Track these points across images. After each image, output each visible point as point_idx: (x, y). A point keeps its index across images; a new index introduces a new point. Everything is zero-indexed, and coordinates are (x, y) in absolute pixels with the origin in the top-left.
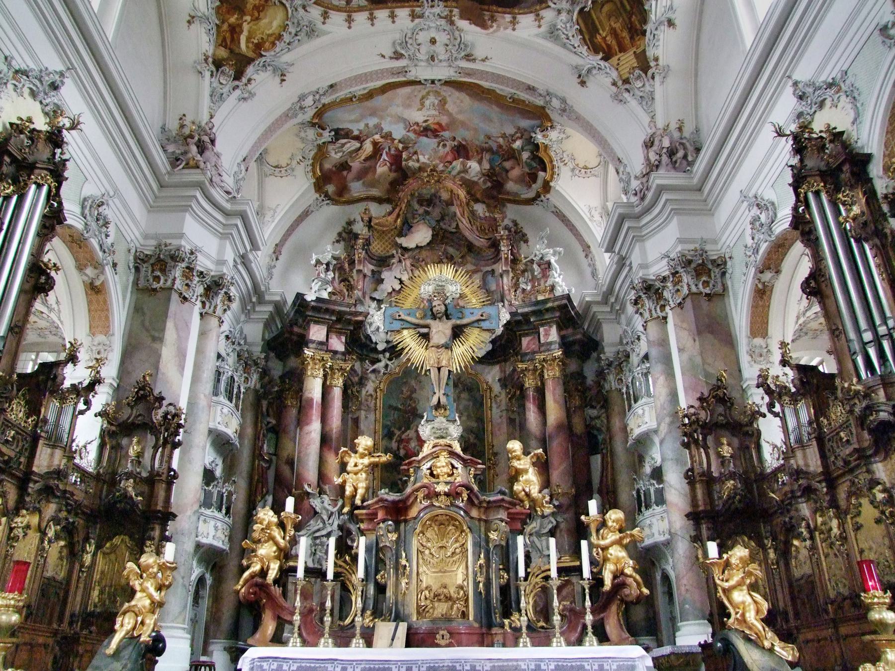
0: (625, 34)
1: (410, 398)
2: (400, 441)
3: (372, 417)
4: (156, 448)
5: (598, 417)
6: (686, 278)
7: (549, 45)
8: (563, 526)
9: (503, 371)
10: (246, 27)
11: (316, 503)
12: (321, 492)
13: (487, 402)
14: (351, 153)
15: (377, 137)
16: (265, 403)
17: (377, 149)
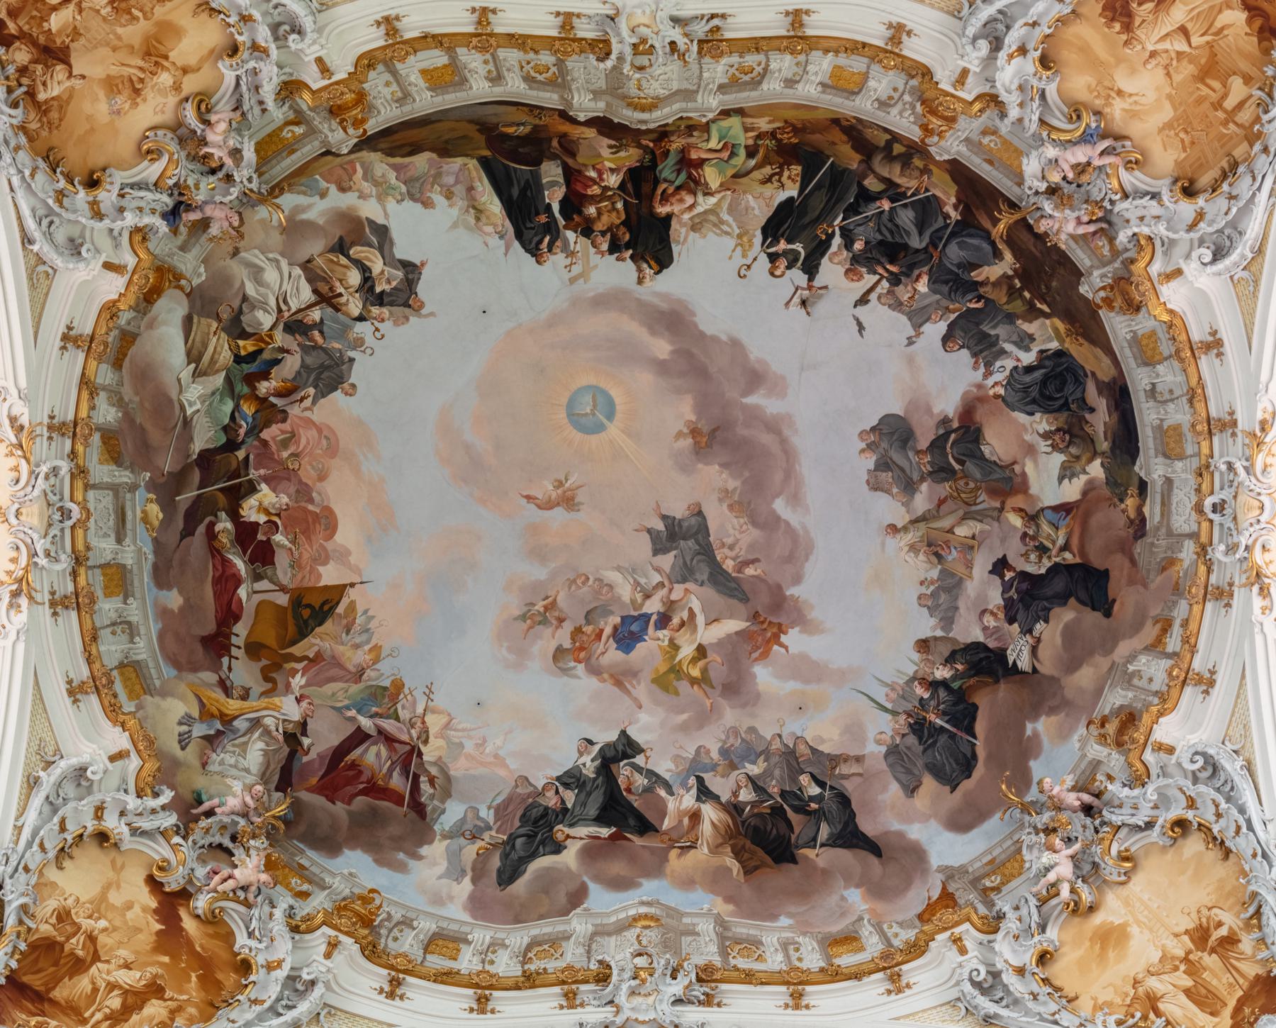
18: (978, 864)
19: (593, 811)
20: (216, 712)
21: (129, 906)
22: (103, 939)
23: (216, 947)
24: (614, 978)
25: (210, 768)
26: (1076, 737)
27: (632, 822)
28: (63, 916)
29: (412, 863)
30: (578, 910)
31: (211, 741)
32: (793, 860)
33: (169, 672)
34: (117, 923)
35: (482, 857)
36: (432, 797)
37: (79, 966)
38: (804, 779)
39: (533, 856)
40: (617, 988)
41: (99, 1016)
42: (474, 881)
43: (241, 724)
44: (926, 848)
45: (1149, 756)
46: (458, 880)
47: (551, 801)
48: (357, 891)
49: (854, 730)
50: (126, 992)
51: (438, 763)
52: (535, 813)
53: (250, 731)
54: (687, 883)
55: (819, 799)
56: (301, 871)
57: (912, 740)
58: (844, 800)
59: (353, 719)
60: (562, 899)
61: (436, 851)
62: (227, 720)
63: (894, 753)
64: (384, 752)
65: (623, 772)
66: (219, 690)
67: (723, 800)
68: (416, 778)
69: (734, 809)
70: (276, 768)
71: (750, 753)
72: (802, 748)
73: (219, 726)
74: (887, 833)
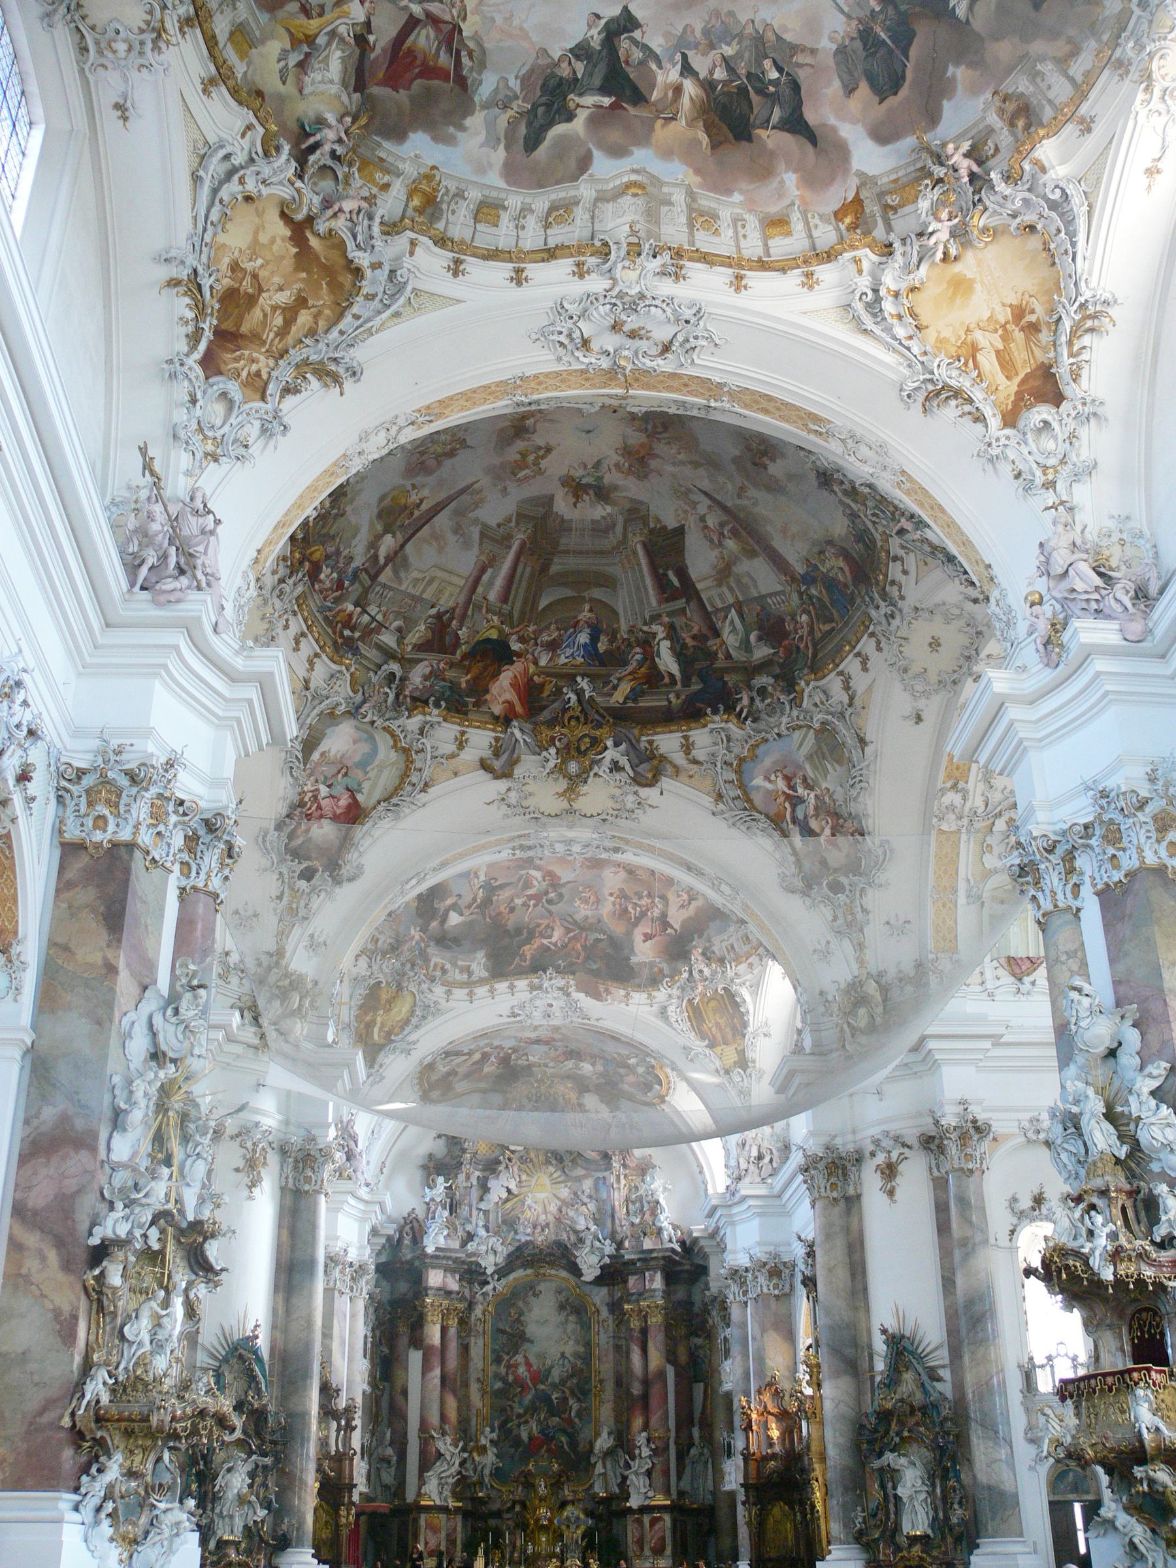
0: (728, 1030)
1: (518, 1320)
2: (509, 1367)
3: (480, 1342)
4: (338, 1431)
5: (701, 1347)
6: (762, 1280)
7: (660, 1023)
8: (658, 1467)
9: (611, 1295)
10: (379, 1019)
11: (440, 1445)
12: (444, 1434)
13: (595, 1327)
14: (458, 1065)
15: (487, 1049)
16: (378, 1333)
17: (485, 1056)
18: (885, 180)
19: (597, 81)
20: (301, 36)
21: (273, 241)
22: (263, 274)
23: (335, 255)
24: (613, 256)
25: (306, 91)
26: (982, 99)
27: (628, 92)
28: (235, 267)
29: (460, 135)
30: (585, 176)
31: (302, 65)
32: (749, 139)
33: (263, 18)
34: (268, 258)
35: (512, 124)
36: (471, 69)
37: (252, 300)
38: (767, 64)
39: (551, 124)
40: (615, 263)
41: (272, 335)
42: (507, 148)
43: (321, 40)
44: (851, 147)
45: (1027, 166)
46: (495, 148)
47: (564, 71)
48: (422, 171)
49: (813, 24)
50: (284, 309)
51: (476, 37)
52: (553, 82)
53: (329, 44)
54: (667, 154)
55: (776, 83)
56: (382, 165)
57: (858, 44)
58: (796, 87)
59: (406, 8)
60: (572, 163)
61: (476, 121)
62: (310, 40)
63: (841, 51)
64: (432, 34)
65: (624, 44)
66: (302, 16)
67: (701, 77)
68: (458, 53)
69: (708, 85)
70: (352, 71)
71: (727, 36)
72: (770, 35)
73: (306, 49)
74: (825, 125)
